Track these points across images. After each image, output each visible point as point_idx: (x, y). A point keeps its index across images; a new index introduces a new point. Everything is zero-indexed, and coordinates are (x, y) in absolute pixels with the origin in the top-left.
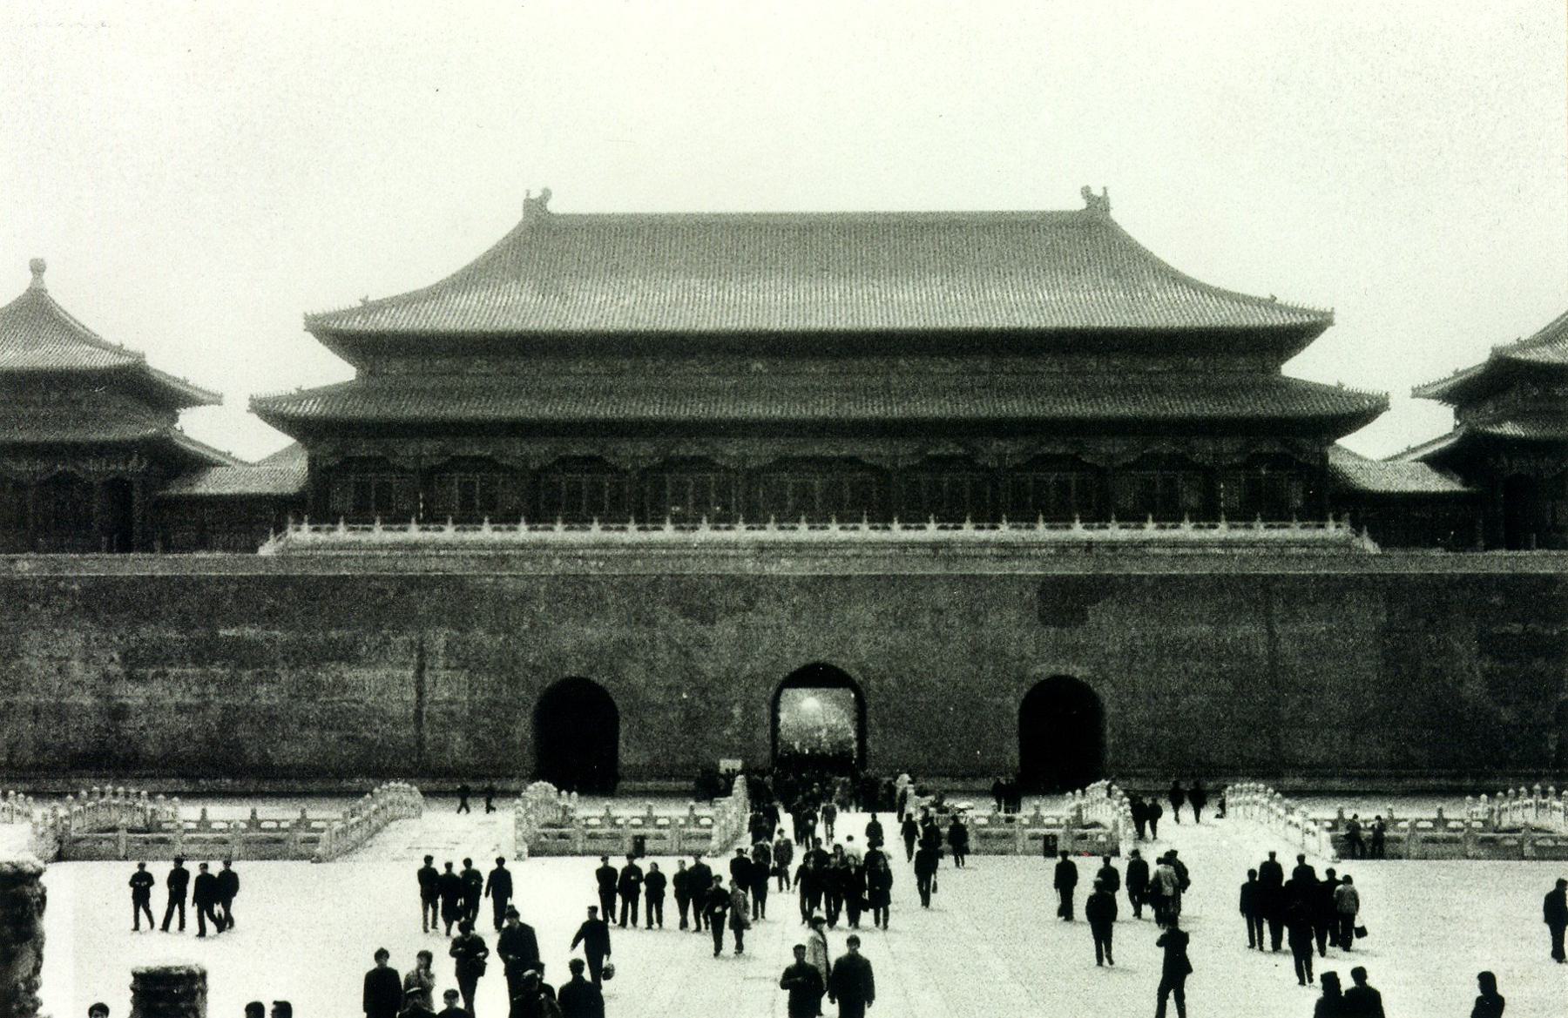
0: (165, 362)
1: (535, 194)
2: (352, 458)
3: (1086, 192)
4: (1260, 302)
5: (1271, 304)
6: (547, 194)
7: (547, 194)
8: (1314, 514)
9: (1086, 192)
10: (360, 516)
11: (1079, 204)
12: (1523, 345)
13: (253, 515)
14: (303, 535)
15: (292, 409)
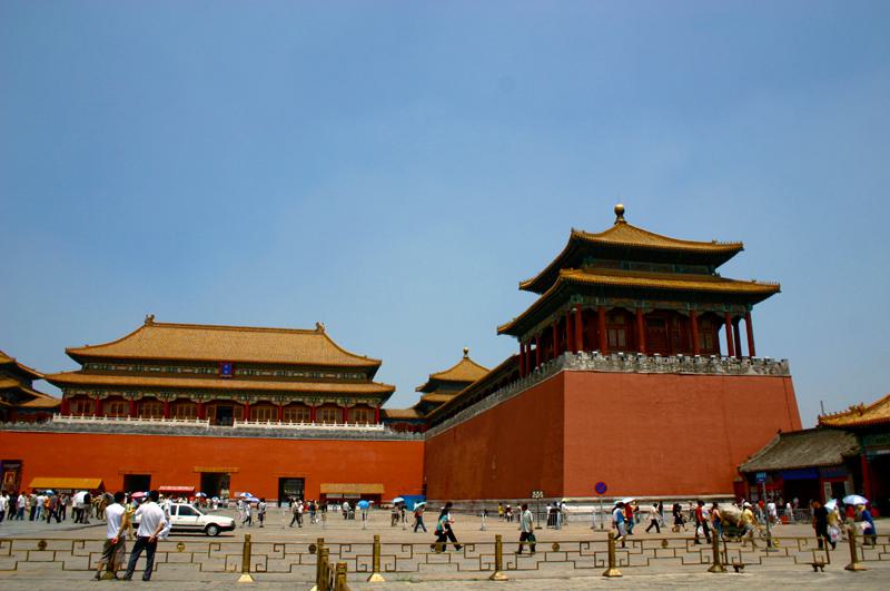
0: (26, 361)
1: (150, 316)
2: (78, 399)
3: (317, 324)
4: (361, 358)
5: (365, 358)
6: (153, 316)
7: (153, 316)
8: (374, 423)
9: (317, 324)
10: (78, 414)
11: (315, 328)
12: (439, 374)
13: (43, 414)
14: (58, 418)
15: (58, 378)
